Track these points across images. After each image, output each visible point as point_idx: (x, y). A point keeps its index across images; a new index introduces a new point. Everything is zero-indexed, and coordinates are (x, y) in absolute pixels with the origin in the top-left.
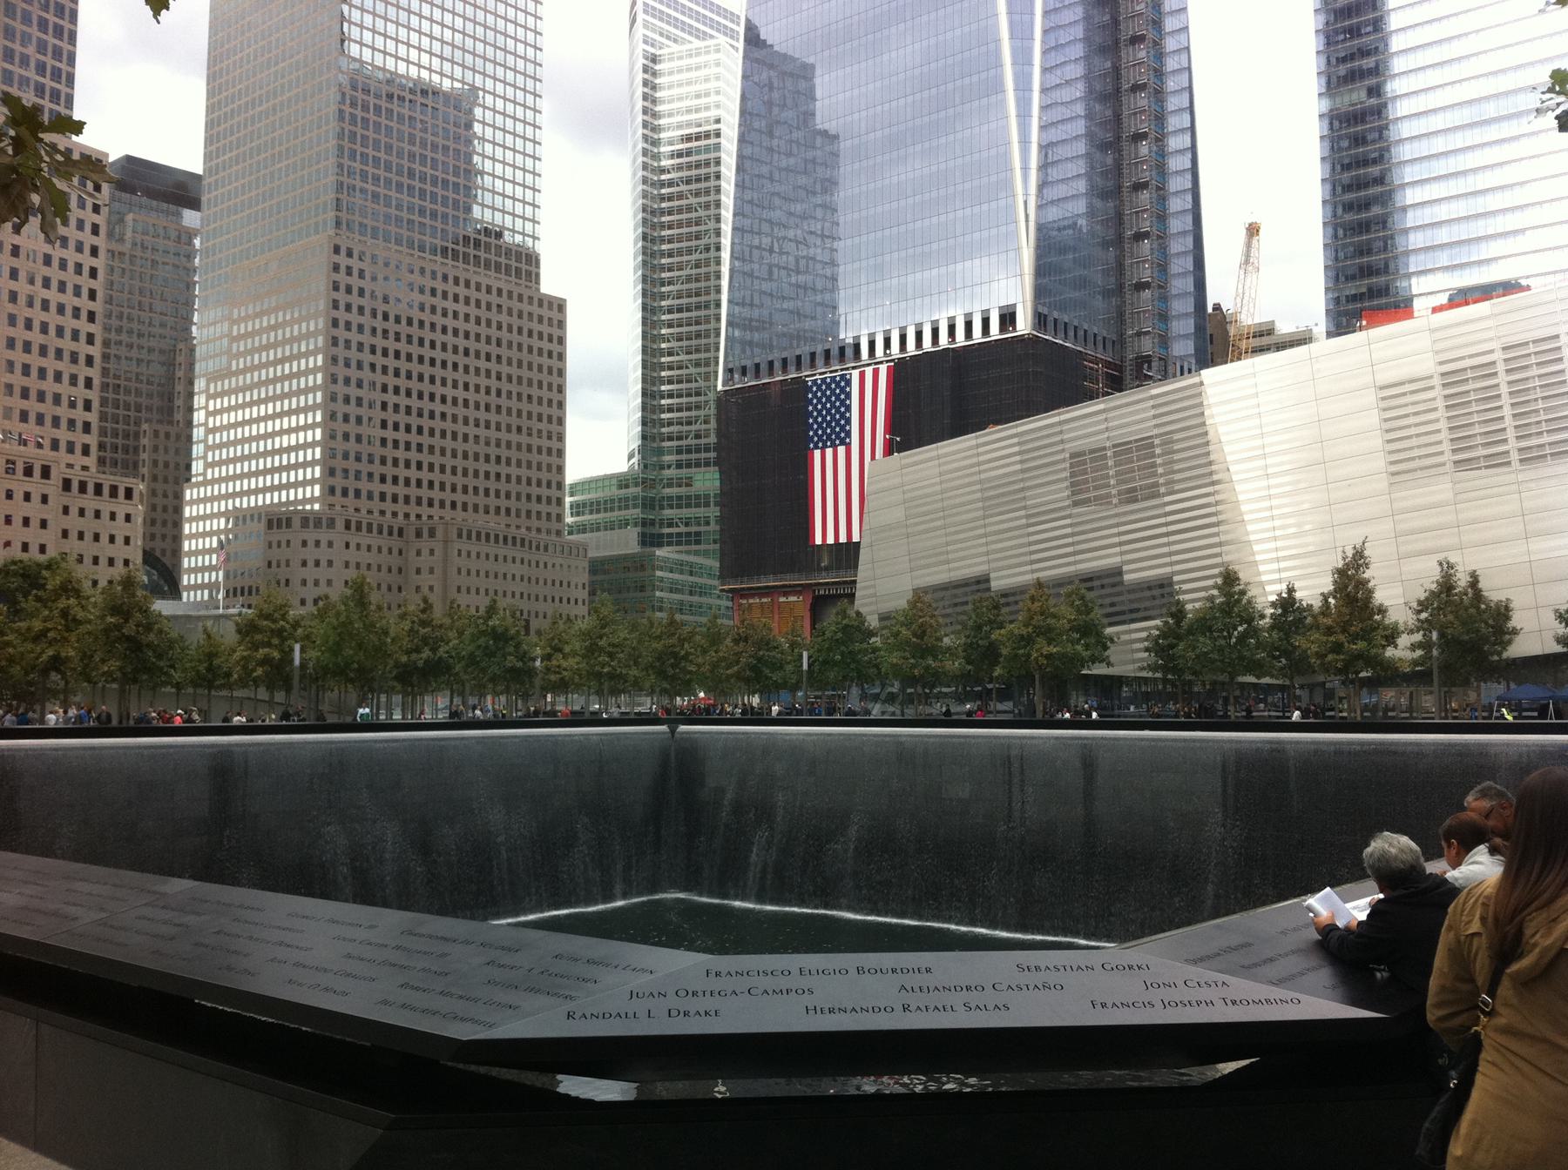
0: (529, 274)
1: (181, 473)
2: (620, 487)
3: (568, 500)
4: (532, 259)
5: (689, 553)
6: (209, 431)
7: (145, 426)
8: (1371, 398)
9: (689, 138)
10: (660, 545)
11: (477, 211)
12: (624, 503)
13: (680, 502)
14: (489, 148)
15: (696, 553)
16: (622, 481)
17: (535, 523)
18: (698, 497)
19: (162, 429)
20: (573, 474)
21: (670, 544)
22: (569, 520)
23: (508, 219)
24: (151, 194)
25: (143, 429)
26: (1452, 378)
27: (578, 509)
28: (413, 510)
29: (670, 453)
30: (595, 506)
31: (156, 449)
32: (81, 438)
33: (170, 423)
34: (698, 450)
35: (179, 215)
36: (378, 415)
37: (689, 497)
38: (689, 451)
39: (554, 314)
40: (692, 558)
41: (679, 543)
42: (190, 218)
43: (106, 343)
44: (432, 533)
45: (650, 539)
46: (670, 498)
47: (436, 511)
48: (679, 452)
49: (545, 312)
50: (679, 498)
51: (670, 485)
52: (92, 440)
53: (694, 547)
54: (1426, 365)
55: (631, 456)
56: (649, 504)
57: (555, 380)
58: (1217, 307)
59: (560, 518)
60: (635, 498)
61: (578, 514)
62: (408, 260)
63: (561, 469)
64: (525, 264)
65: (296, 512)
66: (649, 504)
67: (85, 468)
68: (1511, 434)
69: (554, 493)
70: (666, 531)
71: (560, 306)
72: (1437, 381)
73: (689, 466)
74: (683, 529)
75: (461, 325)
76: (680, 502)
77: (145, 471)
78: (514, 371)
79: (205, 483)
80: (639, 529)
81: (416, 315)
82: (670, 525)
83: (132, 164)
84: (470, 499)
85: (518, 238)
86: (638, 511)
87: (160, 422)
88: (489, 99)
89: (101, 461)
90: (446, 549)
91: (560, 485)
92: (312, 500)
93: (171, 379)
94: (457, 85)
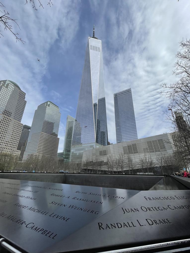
4: (57, 135)
6: (28, 147)
8: (122, 148)
17: (54, 156)
24: (26, 128)
26: (128, 146)
27: (58, 155)
30: (60, 155)
32: (16, 147)
35: (29, 130)
36: (42, 146)
42: (30, 130)
43: (20, 139)
54: (126, 145)
63: (57, 152)
64: (57, 135)
68: (133, 151)
69: (56, 154)
71: (59, 139)
72: (127, 147)
78: (54, 143)
81: (47, 139)
83: (25, 125)
89: (17, 149)
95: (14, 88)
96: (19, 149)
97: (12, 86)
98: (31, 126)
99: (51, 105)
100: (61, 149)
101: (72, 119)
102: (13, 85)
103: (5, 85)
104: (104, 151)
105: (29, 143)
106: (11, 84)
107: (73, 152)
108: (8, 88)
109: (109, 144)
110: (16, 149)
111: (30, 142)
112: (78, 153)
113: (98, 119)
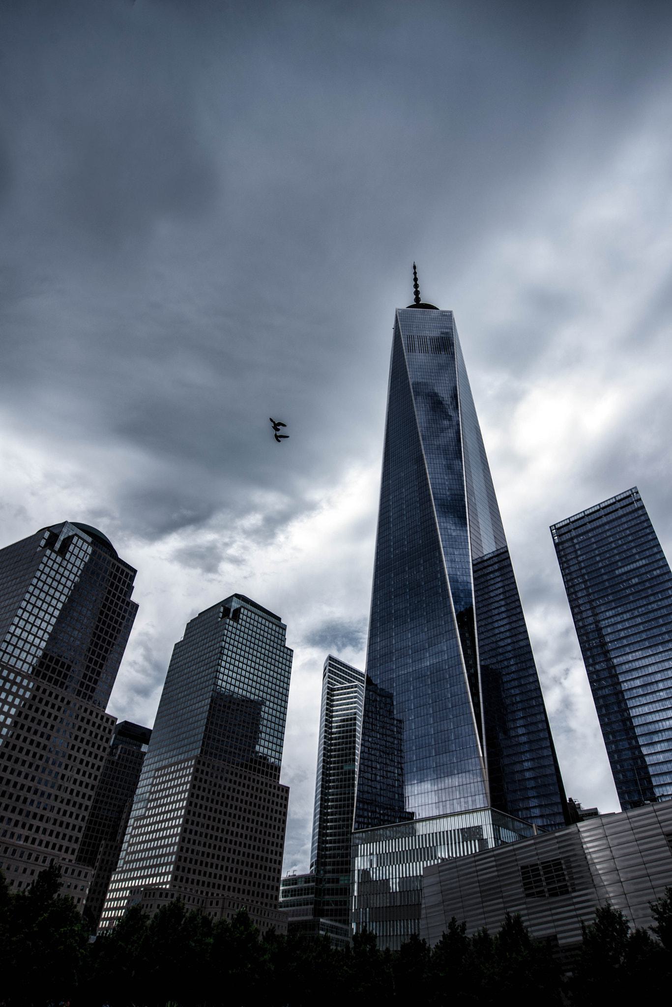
0: (275, 775)
1: (112, 867)
2: (306, 882)
3: (281, 888)
5: (336, 921)
7: (103, 842)
9: (343, 721)
10: (322, 916)
11: (257, 747)
12: (306, 891)
13: (331, 892)
14: (265, 722)
15: (340, 921)
16: (306, 878)
18: (341, 889)
19: (110, 843)
20: (284, 875)
21: (327, 916)
22: (281, 899)
23: (270, 752)
25: (102, 840)
28: (211, 890)
29: (329, 865)
30: (293, 893)
31: (105, 854)
33: (114, 841)
34: (342, 864)
37: (337, 889)
38: (338, 865)
39: (284, 794)
40: (337, 924)
41: (331, 915)
44: (217, 904)
45: (319, 912)
46: (328, 890)
47: (220, 892)
48: (334, 865)
49: (280, 793)
50: (333, 889)
51: (329, 882)
52: (77, 846)
53: (338, 918)
55: (311, 866)
56: (318, 892)
57: (281, 825)
58: (571, 800)
59: (277, 898)
60: (312, 888)
61: (285, 896)
62: (227, 768)
63: (279, 872)
65: (159, 889)
66: (318, 892)
67: (70, 861)
70: (326, 907)
71: (286, 790)
73: (338, 872)
74: (333, 907)
75: (244, 798)
76: (331, 892)
77: (97, 864)
79: (121, 872)
80: (312, 906)
82: (328, 905)
83: (126, 723)
84: (237, 885)
85: (273, 760)
86: (313, 896)
87: (110, 840)
88: (268, 703)
89: (79, 859)
90: (222, 912)
91: (279, 879)
92: (166, 883)
93: (120, 819)
94: (256, 697)
95: (90, 551)
96: (86, 857)
97: (85, 546)
98: (150, 725)
99: (246, 612)
100: (298, 858)
101: (346, 673)
102: (90, 540)
103: (58, 546)
104: (546, 866)
105: (137, 819)
106: (80, 537)
107: (365, 873)
108: (68, 556)
109: (573, 814)
110: (73, 857)
111: (144, 817)
112: (394, 875)
113: (483, 663)
